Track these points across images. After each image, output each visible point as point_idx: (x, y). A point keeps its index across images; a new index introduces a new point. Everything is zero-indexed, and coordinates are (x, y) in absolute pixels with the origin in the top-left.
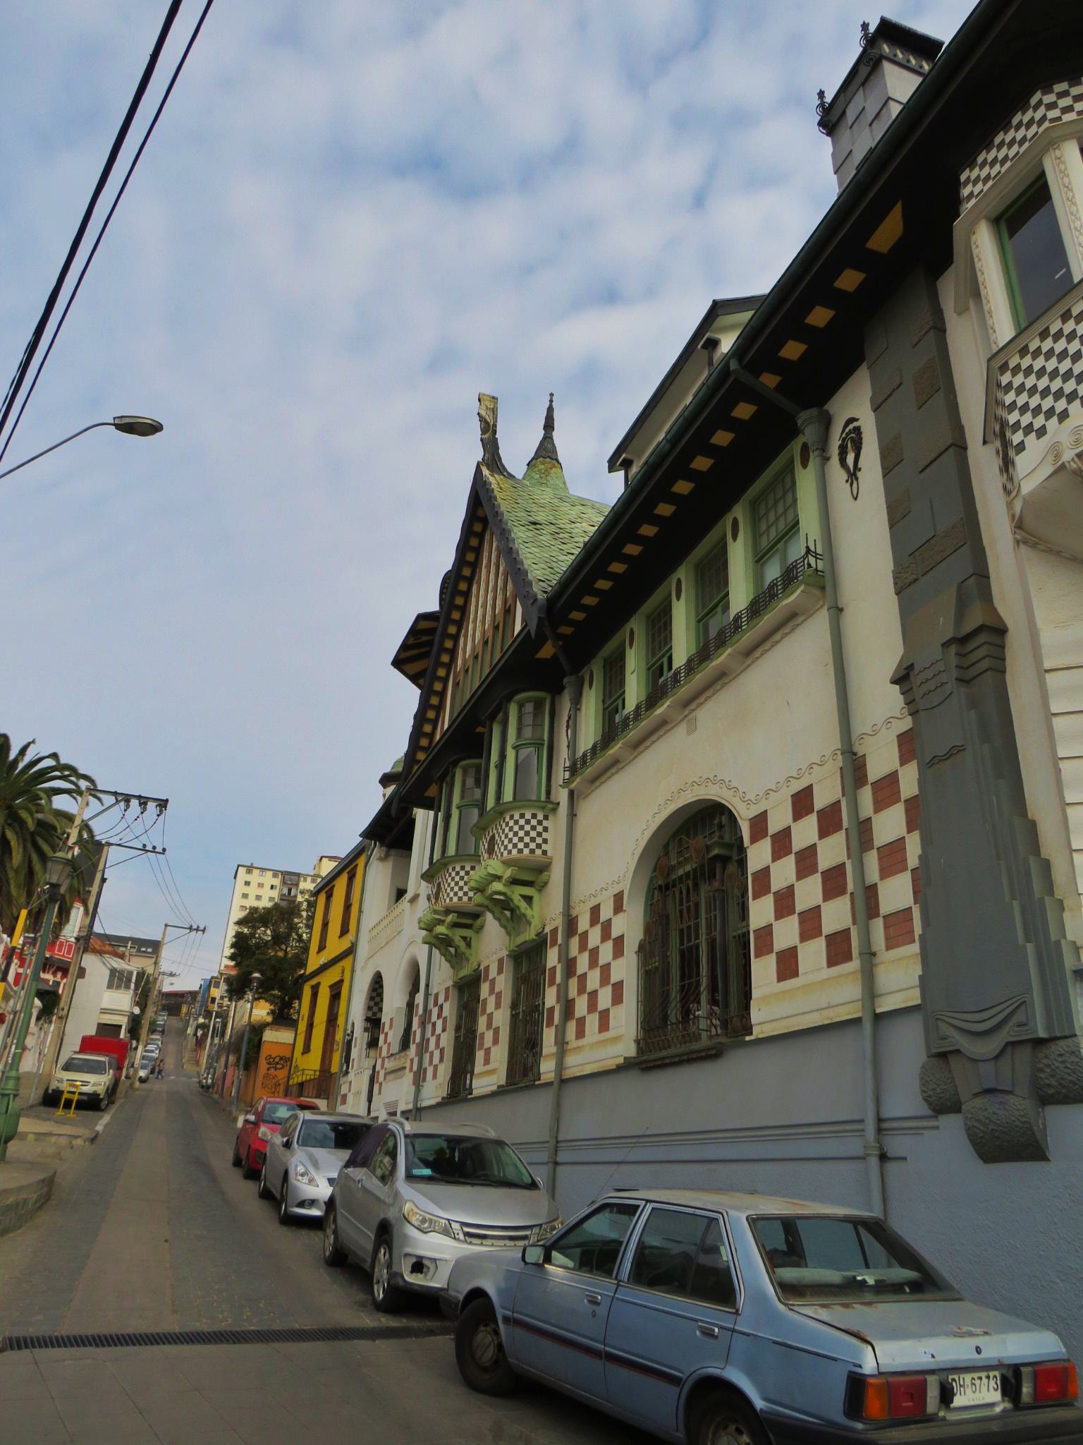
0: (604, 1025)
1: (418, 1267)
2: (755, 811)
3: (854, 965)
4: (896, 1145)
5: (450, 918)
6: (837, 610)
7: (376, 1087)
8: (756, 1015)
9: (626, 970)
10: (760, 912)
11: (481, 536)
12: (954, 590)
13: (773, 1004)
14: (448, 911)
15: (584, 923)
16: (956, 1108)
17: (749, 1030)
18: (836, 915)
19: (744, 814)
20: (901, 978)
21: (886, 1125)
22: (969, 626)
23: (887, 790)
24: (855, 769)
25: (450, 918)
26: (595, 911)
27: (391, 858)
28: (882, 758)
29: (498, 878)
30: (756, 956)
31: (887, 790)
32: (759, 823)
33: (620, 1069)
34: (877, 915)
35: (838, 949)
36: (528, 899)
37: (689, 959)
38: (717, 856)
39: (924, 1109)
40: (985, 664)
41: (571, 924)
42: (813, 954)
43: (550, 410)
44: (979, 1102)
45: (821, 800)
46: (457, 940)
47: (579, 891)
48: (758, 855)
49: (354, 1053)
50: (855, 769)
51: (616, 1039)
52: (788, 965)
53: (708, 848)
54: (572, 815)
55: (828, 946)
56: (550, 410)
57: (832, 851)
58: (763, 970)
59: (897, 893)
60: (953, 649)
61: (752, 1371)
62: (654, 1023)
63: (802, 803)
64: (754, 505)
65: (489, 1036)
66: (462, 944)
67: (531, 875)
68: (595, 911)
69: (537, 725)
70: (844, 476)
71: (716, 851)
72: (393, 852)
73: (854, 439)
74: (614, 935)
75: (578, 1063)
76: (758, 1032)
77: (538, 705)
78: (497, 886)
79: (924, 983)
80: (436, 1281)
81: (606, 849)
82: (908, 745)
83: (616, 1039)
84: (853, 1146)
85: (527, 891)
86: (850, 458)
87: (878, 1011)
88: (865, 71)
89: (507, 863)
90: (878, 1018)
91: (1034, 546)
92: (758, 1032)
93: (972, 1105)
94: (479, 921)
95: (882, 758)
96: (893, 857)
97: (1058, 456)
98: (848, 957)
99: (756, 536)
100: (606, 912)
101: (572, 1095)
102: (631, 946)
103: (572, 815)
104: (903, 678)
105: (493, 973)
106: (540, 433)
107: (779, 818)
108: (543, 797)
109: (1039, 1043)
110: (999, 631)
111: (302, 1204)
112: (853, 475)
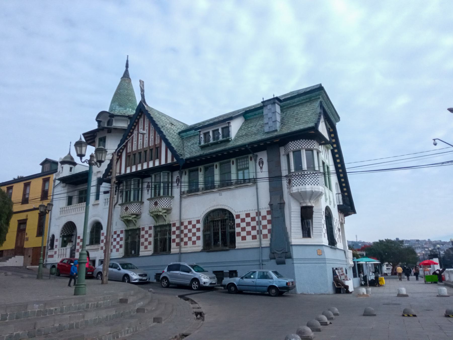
0: (194, 243)
1: (205, 283)
2: (237, 214)
4: (264, 263)
5: (134, 216)
6: (257, 189)
8: (237, 245)
9: (200, 234)
10: (238, 230)
11: (138, 120)
14: (132, 214)
15: (186, 223)
16: (275, 259)
18: (254, 233)
19: (234, 214)
20: (266, 243)
23: (264, 218)
24: (258, 214)
25: (134, 216)
26: (190, 223)
28: (264, 213)
29: (160, 212)
30: (237, 236)
31: (264, 218)
35: (254, 237)
36: (166, 216)
37: (216, 234)
41: (182, 224)
42: (249, 238)
43: (127, 61)
46: (134, 221)
47: (184, 217)
48: (237, 221)
49: (56, 243)
50: (258, 214)
51: (199, 246)
52: (244, 238)
54: (181, 201)
56: (127, 61)
57: (253, 224)
59: (265, 232)
61: (276, 284)
63: (248, 215)
64: (237, 160)
65: (146, 243)
66: (135, 222)
67: (168, 211)
68: (190, 223)
69: (168, 179)
70: (259, 167)
72: (67, 185)
73: (261, 162)
75: (184, 250)
76: (237, 248)
77: (168, 173)
78: (161, 214)
79: (270, 244)
80: (207, 285)
81: (192, 210)
82: (268, 213)
83: (199, 246)
84: (258, 263)
85: (166, 214)
86: (261, 165)
89: (164, 209)
90: (262, 247)
94: (139, 217)
95: (264, 213)
96: (265, 227)
98: (256, 238)
99: (237, 166)
100: (194, 222)
101: (183, 256)
102: (201, 229)
103: (181, 201)
105: (147, 229)
106: (124, 69)
107: (243, 216)
108: (170, 195)
110: (284, 203)
111: (134, 280)
112: (261, 168)
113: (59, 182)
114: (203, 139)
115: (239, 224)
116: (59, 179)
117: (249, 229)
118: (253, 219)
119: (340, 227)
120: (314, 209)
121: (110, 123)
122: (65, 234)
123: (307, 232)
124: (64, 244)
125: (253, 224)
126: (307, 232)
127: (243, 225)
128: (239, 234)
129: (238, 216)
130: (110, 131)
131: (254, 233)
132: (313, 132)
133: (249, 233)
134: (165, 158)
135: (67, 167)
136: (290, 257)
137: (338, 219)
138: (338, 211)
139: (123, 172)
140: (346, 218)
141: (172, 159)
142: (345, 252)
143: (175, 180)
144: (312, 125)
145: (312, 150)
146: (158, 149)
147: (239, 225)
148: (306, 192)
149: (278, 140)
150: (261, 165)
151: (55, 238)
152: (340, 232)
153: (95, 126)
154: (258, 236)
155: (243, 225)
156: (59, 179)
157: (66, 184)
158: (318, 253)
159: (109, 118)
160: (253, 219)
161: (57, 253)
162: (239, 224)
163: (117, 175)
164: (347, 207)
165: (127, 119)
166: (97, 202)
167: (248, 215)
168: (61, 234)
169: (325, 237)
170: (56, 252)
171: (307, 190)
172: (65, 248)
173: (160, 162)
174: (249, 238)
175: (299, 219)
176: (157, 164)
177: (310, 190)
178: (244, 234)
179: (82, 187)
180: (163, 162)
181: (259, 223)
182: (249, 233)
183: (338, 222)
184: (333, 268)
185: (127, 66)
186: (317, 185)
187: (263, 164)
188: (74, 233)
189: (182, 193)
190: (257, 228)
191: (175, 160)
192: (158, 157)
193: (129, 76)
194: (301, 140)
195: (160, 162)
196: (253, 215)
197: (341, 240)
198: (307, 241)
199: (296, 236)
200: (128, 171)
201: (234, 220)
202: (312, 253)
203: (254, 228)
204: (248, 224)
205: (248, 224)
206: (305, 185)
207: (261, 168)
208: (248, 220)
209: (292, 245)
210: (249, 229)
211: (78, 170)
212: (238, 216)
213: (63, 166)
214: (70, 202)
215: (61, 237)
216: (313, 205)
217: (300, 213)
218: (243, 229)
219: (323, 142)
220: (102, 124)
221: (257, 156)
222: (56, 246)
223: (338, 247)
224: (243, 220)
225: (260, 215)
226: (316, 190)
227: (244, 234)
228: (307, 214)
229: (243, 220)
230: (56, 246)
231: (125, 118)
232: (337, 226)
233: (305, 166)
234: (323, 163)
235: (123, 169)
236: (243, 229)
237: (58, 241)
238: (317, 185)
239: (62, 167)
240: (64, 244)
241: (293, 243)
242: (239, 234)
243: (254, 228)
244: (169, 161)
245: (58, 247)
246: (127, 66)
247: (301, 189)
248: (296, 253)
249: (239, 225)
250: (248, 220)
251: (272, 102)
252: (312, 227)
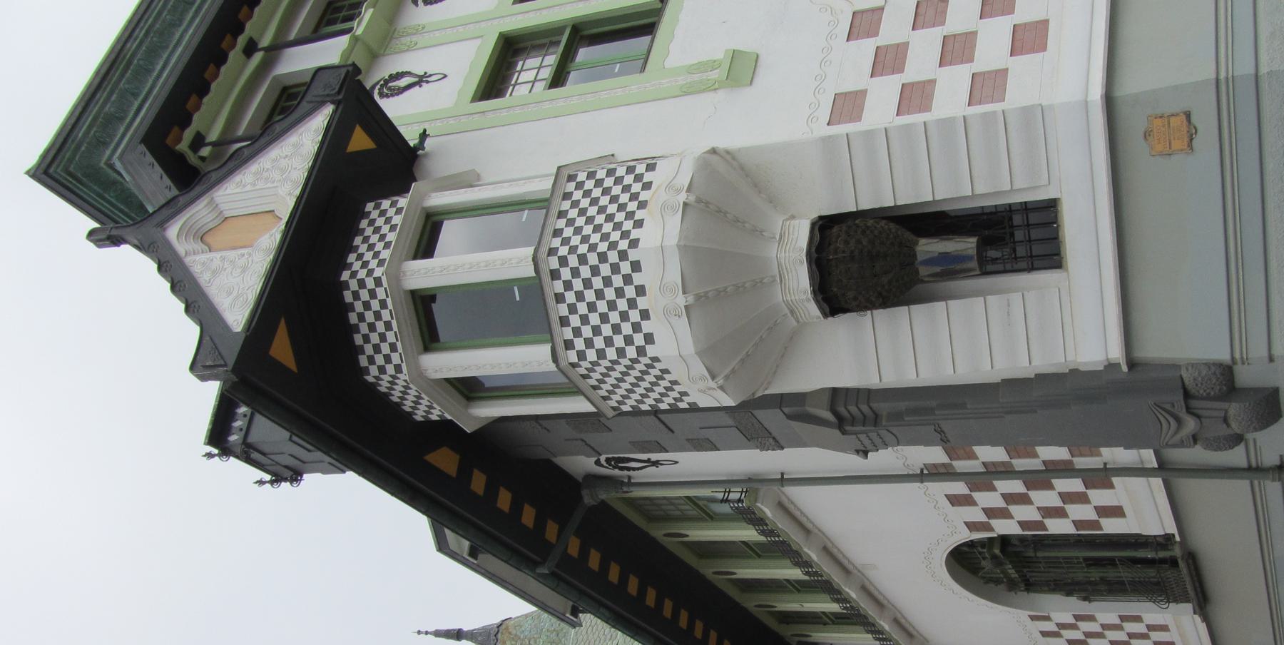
3: (1115, 480)
10: (1057, 527)
12: (793, 423)
17: (1168, 538)
19: (965, 536)
21: (1254, 464)
22: (828, 415)
32: (972, 526)
33: (1206, 619)
34: (1070, 462)
38: (1002, 551)
39: (1242, 446)
40: (865, 408)
44: (1234, 425)
45: (960, 488)
53: (994, 557)
55: (1095, 487)
58: (1111, 526)
60: (848, 428)
62: (1161, 591)
71: (997, 551)
74: (1073, 621)
76: (1171, 528)
87: (1156, 466)
88: (249, 454)
91: (769, 383)
92: (1171, 528)
93: (1236, 427)
97: (710, 389)
104: (865, 454)
109: (1187, 395)
123: (1014, 237)
126: (1014, 237)
132: (282, 349)
136: (1226, 372)
148: (711, 353)
171: (689, 347)
177: (682, 324)
198: (1086, 230)
199: (1062, 322)
202: (1185, 191)
206: (655, 359)
209: (1132, 364)
217: (879, 313)
219: (360, 141)
226: (674, 276)
241: (1116, 352)
247: (692, 380)
248: (1191, 335)
252: (973, 196)
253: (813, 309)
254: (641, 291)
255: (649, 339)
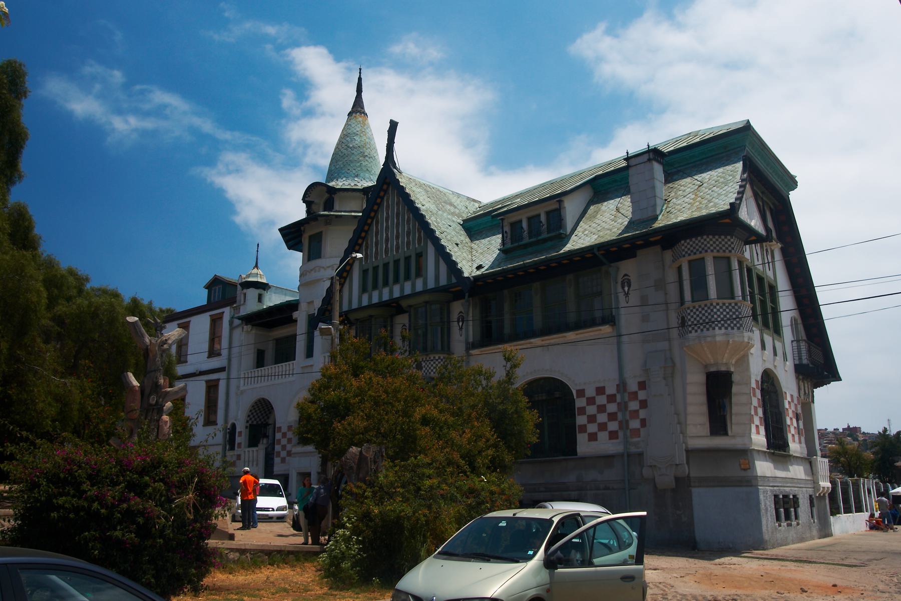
2: (578, 388)
7: (277, 460)
8: (579, 450)
10: (581, 420)
13: (584, 446)
17: (574, 452)
18: (613, 426)
24: (622, 386)
27: (254, 332)
42: (603, 436)
43: (360, 79)
48: (580, 403)
49: (238, 440)
52: (593, 437)
56: (360, 79)
57: (612, 408)
63: (600, 391)
86: (626, 289)
98: (617, 438)
107: (590, 392)
112: (627, 295)
113: (240, 322)
114: (509, 237)
115: (584, 408)
116: (239, 318)
117: (602, 418)
118: (611, 399)
119: (800, 411)
120: (735, 378)
121: (329, 206)
122: (255, 423)
123: (719, 421)
124: (253, 442)
125: (612, 408)
127: (591, 410)
128: (583, 429)
129: (581, 393)
130: (329, 220)
131: (613, 426)
132: (727, 221)
133: (603, 427)
134: (433, 275)
135: (252, 293)
137: (796, 395)
138: (797, 378)
139: (355, 305)
140: (818, 392)
141: (449, 278)
142: (810, 463)
143: (455, 316)
144: (724, 206)
145: (728, 259)
146: (420, 256)
147: (582, 411)
149: (659, 238)
150: (626, 289)
151: (238, 430)
152: (801, 423)
153: (299, 212)
154: (621, 434)
155: (591, 410)
156: (239, 318)
157: (253, 325)
158: (743, 466)
159: (327, 195)
160: (611, 399)
161: (242, 457)
162: (584, 408)
163: (345, 308)
164: (819, 367)
165: (361, 195)
166: (309, 362)
167: (600, 391)
168: (247, 422)
169: (758, 433)
170: (239, 457)
172: (255, 449)
173: (425, 283)
174: (603, 436)
175: (703, 399)
176: (419, 287)
178: (592, 428)
179: (282, 332)
180: (431, 284)
181: (623, 406)
182: (603, 427)
183: (796, 401)
184: (776, 496)
185: (359, 90)
186: (739, 328)
187: (629, 286)
188: (270, 421)
189: (471, 346)
190: (620, 416)
191: (454, 280)
192: (419, 274)
193: (363, 108)
194: (705, 237)
195: (425, 283)
196: (611, 390)
197: (803, 439)
200: (365, 302)
201: (573, 402)
203: (612, 417)
204: (602, 409)
205: (602, 409)
206: (714, 329)
207: (627, 295)
208: (601, 400)
210: (602, 418)
211: (272, 300)
212: (581, 393)
213: (245, 291)
214: (260, 362)
215: (246, 427)
216: (732, 369)
218: (592, 419)
219: (753, 238)
220: (314, 207)
221: (618, 269)
222: (240, 444)
223: (791, 453)
224: (591, 401)
225: (625, 390)
227: (592, 428)
228: (719, 386)
229: (591, 401)
230: (240, 444)
231: (358, 194)
232: (793, 408)
233: (713, 292)
234: (760, 279)
235: (354, 296)
236: (592, 419)
237: (243, 434)
238: (739, 328)
239: (245, 294)
240: (253, 442)
242: (583, 429)
243: (612, 417)
244: (443, 281)
245: (243, 446)
246: (359, 90)
249: (582, 411)
250: (601, 400)
251: (646, 157)
253: (713, 369)
254: (733, 328)
255: (720, 328)
